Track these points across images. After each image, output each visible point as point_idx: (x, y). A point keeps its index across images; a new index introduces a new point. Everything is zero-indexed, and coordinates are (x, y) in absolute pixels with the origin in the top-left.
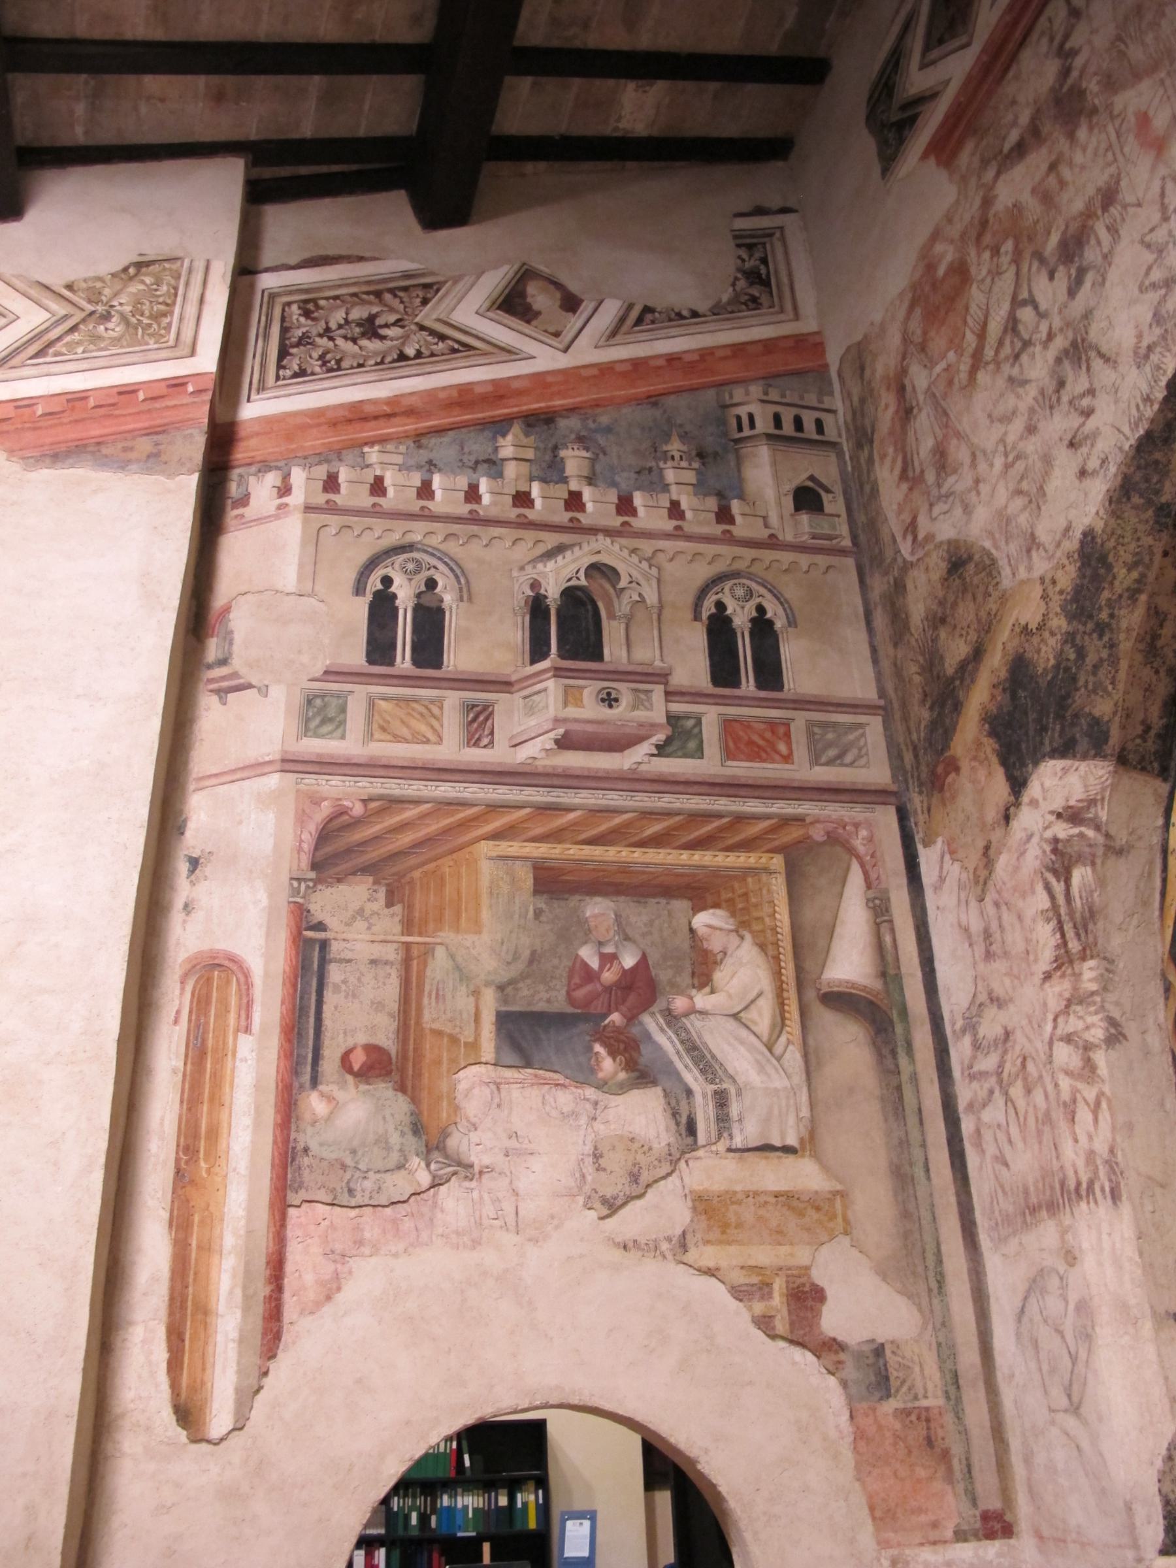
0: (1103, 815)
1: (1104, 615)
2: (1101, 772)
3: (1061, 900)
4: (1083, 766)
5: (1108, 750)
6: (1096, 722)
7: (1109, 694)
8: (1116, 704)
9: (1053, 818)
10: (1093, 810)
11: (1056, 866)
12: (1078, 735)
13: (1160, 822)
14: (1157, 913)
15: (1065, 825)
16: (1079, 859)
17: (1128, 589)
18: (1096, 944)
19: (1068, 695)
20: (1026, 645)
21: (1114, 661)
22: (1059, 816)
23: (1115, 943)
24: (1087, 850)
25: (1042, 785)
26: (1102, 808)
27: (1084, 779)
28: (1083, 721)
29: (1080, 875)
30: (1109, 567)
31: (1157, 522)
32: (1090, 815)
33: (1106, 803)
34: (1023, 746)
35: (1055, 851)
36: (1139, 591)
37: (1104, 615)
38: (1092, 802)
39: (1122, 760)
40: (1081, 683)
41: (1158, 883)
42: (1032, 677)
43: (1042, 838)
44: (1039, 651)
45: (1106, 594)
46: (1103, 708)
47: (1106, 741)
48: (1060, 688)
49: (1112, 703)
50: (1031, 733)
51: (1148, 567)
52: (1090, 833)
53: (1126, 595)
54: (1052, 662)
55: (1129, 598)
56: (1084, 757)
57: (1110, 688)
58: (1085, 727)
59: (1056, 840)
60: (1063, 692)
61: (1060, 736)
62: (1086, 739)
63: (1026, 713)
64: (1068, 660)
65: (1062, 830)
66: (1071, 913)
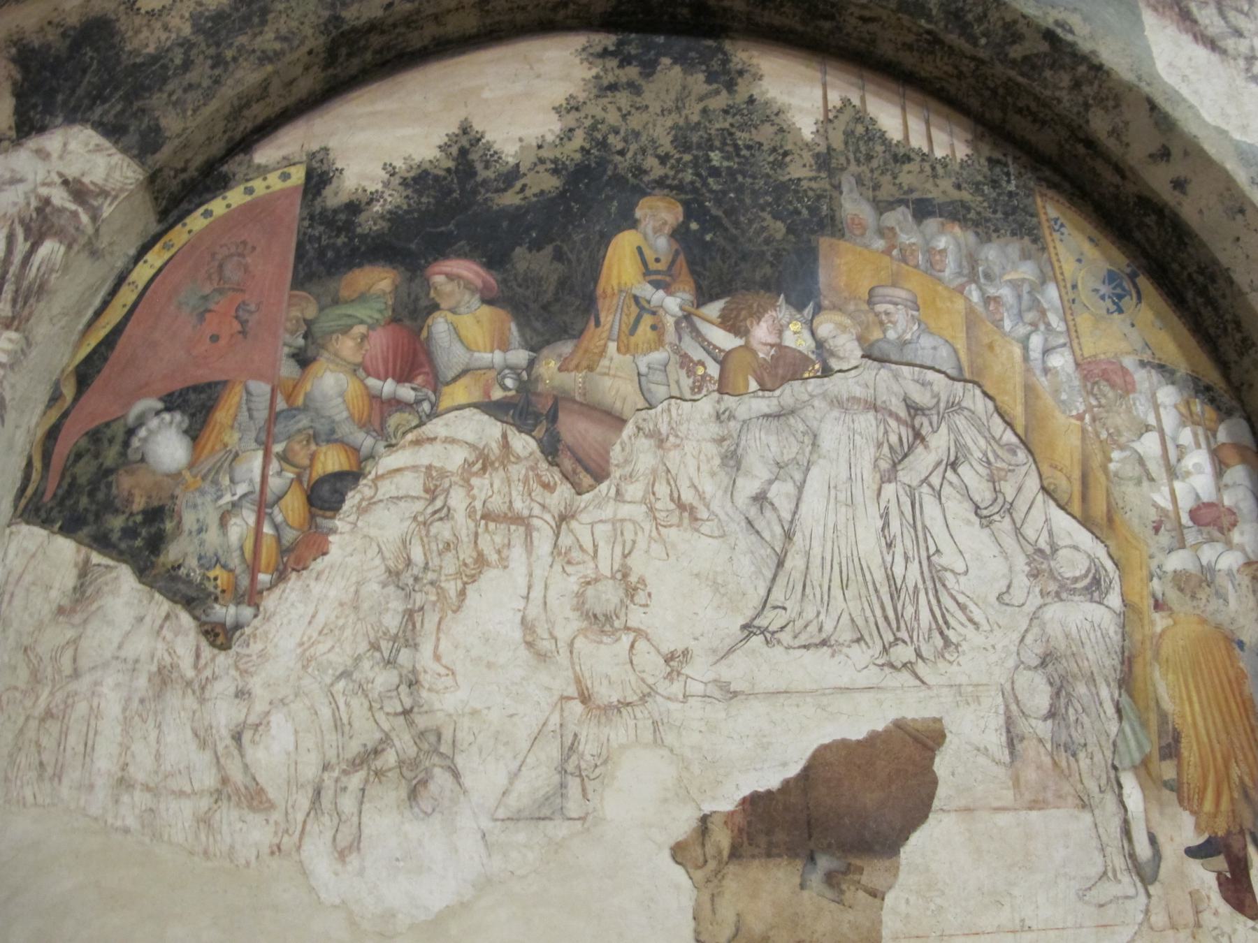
0: (107, 211)
1: (229, 54)
2: (130, 174)
3: (17, 258)
4: (118, 158)
5: (150, 160)
6: (157, 129)
7: (184, 117)
8: (184, 129)
9: (58, 180)
10: (100, 200)
11: (33, 225)
12: (132, 128)
13: (132, 252)
14: (81, 327)
15: (65, 195)
16: (60, 234)
17: (263, 52)
18: (28, 320)
19: (149, 89)
20: (123, 18)
21: (208, 95)
22: (66, 182)
23: (42, 330)
24: (72, 231)
25: (65, 145)
26: (110, 205)
27: (111, 169)
28: (146, 120)
29: (50, 249)
30: (264, 22)
31: (325, 25)
32: (95, 204)
33: (116, 203)
34: (60, 98)
35: (39, 210)
36: (270, 60)
37: (229, 54)
38: (104, 193)
39: (152, 179)
40: (169, 87)
41: (97, 302)
42: (113, 47)
43: (34, 190)
44: (137, 32)
45: (242, 39)
46: (171, 123)
47: (154, 152)
48: (147, 77)
49: (182, 125)
50: (80, 92)
51: (292, 49)
52: (85, 218)
53: (258, 53)
54: (151, 49)
55: (259, 59)
56: (125, 151)
57: (189, 113)
58: (143, 127)
59: (47, 201)
60: (147, 82)
61: (116, 116)
62: (137, 137)
63: (84, 71)
64: (172, 60)
65: (60, 197)
66: (20, 277)
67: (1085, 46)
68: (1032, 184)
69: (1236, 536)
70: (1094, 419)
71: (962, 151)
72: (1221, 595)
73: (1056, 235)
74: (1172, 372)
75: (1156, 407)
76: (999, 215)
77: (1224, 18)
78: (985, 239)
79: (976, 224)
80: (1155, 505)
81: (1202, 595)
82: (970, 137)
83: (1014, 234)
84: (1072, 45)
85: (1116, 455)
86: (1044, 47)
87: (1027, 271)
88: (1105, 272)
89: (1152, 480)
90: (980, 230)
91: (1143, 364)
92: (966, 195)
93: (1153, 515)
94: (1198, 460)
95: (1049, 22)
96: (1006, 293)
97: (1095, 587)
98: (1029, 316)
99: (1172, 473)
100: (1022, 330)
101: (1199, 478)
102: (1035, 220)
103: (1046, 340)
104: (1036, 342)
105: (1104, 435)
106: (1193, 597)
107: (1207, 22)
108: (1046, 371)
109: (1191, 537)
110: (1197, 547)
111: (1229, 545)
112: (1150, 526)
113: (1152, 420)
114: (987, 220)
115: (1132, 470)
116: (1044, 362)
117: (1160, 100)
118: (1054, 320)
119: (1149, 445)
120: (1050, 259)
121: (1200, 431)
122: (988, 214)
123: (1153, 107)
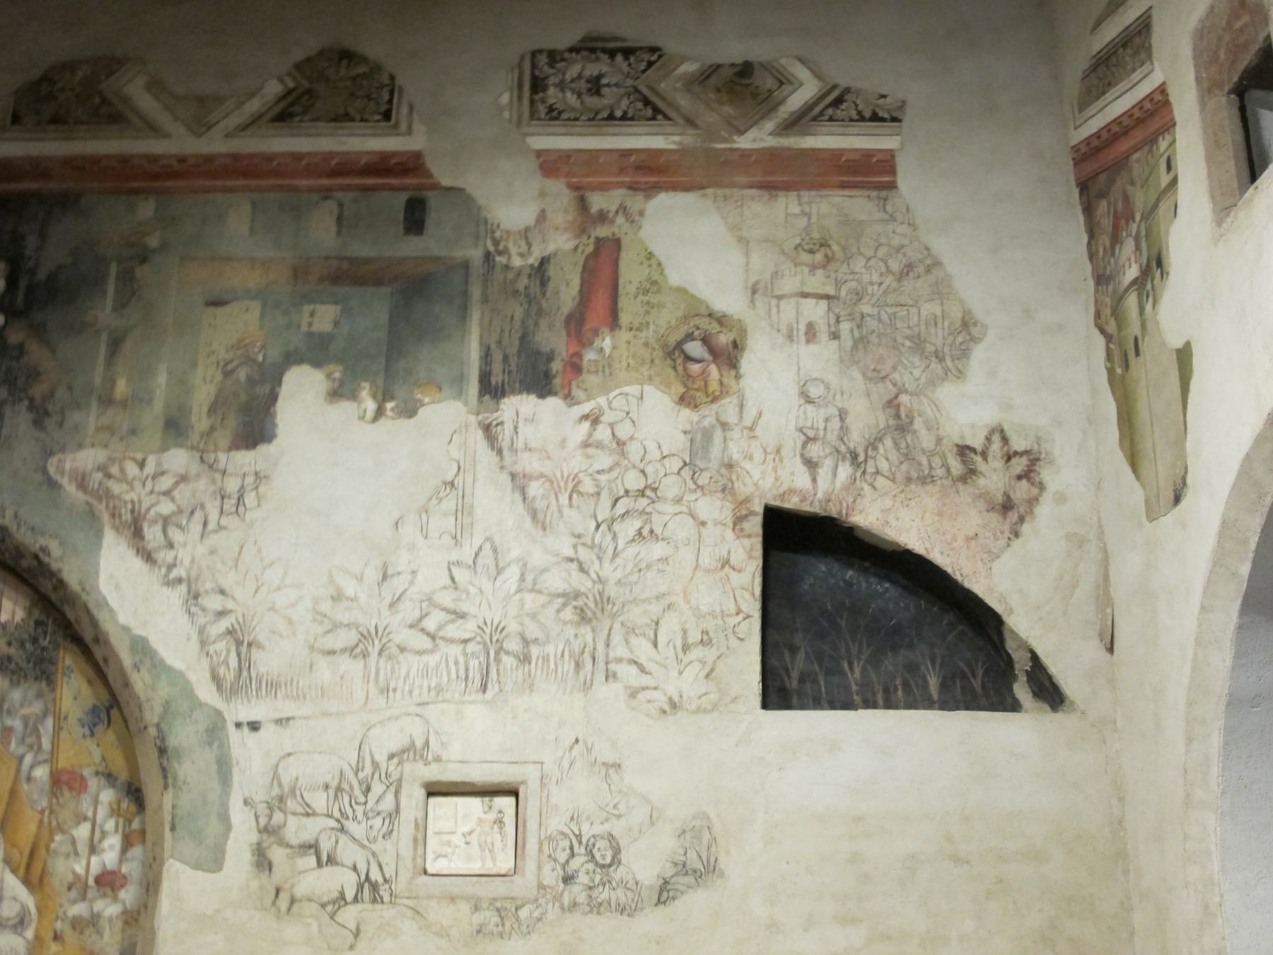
67: (55, 566)
68: (60, 639)
69: (123, 894)
70: (51, 812)
71: (20, 615)
72: (100, 933)
73: (65, 679)
74: (116, 779)
75: (96, 802)
76: (31, 665)
77: (165, 531)
78: (14, 684)
79: (13, 673)
80: (74, 873)
81: (87, 932)
82: (27, 603)
83: (36, 679)
84: (48, 565)
85: (58, 838)
86: (35, 563)
87: (36, 708)
88: (90, 706)
89: (76, 853)
90: (14, 678)
91: (97, 773)
92: (12, 651)
93: (70, 878)
94: (113, 842)
95: (35, 548)
96: (17, 724)
97: (20, 923)
98: (29, 740)
99: (93, 849)
100: (21, 750)
101: (110, 853)
102: (53, 668)
103: (35, 757)
104: (28, 759)
105: (54, 823)
106: (81, 933)
107: (151, 537)
108: (29, 779)
109: (90, 894)
110: (93, 900)
111: (115, 899)
112: (66, 885)
113: (90, 814)
114: (21, 669)
115: (67, 848)
116: (30, 773)
117: (92, 606)
118: (46, 743)
119: (83, 831)
120: (55, 700)
121: (121, 821)
122: (24, 664)
123: (88, 611)
